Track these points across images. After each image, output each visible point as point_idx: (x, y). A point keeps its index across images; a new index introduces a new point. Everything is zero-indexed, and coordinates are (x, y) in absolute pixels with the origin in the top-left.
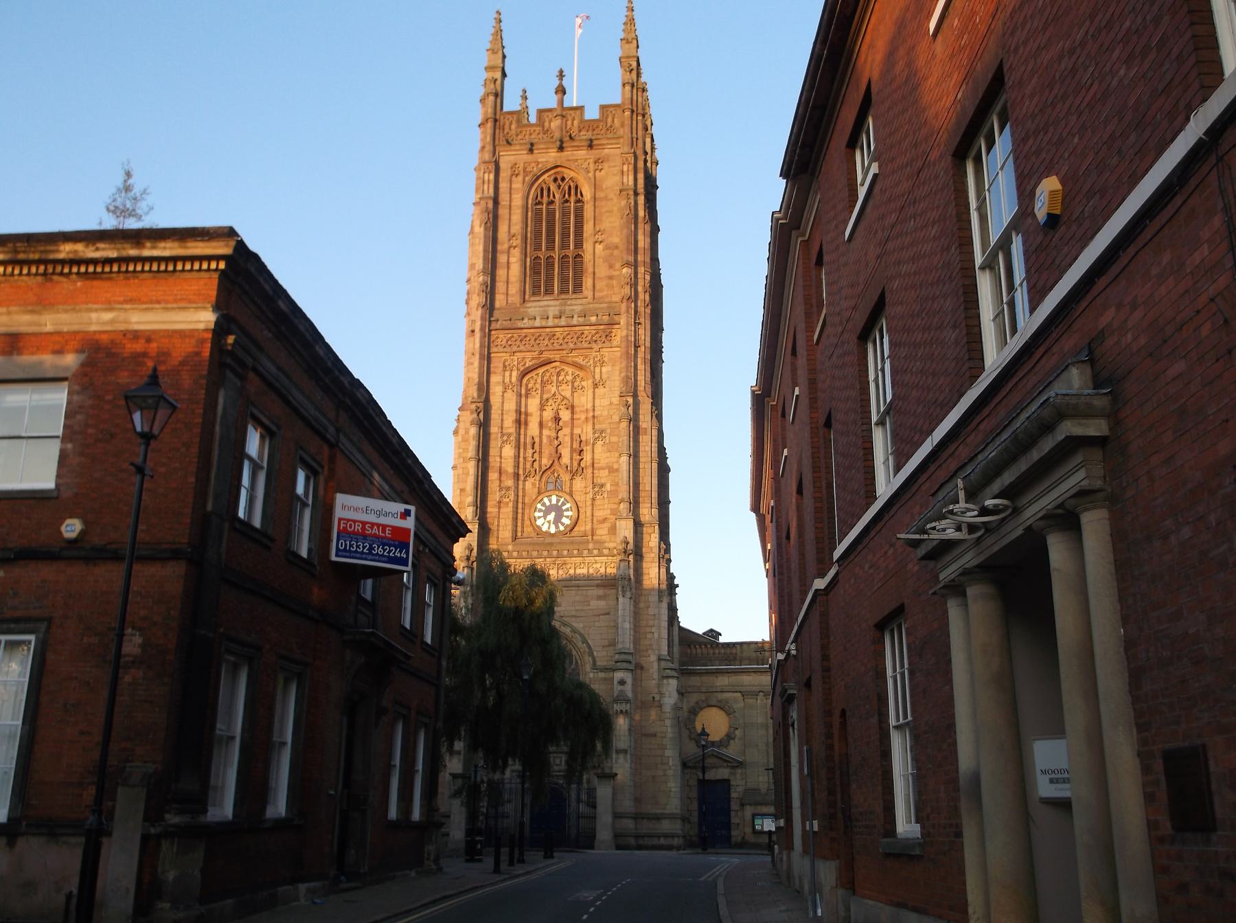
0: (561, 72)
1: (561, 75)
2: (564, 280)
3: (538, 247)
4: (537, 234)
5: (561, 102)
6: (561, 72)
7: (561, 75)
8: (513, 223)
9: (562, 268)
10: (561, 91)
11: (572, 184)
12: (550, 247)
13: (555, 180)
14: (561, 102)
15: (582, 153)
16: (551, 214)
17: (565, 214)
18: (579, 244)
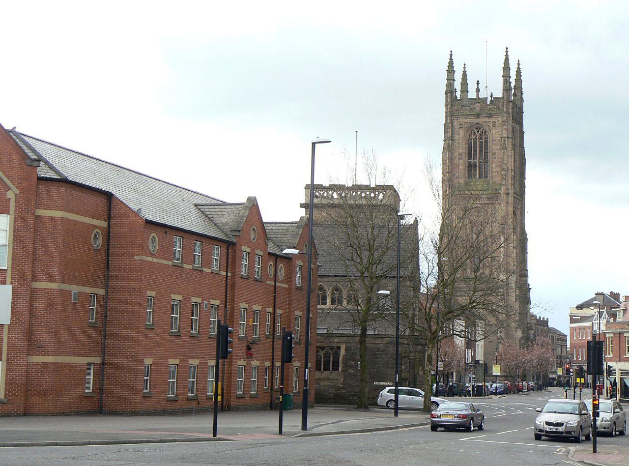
0: (478, 81)
1: (478, 84)
2: (480, 173)
3: (470, 158)
4: (470, 152)
5: (478, 95)
6: (478, 81)
7: (478, 84)
8: (461, 148)
9: (480, 168)
10: (478, 90)
11: (484, 131)
12: (475, 158)
13: (477, 128)
14: (478, 95)
15: (487, 120)
16: (475, 143)
17: (481, 143)
18: (486, 157)
